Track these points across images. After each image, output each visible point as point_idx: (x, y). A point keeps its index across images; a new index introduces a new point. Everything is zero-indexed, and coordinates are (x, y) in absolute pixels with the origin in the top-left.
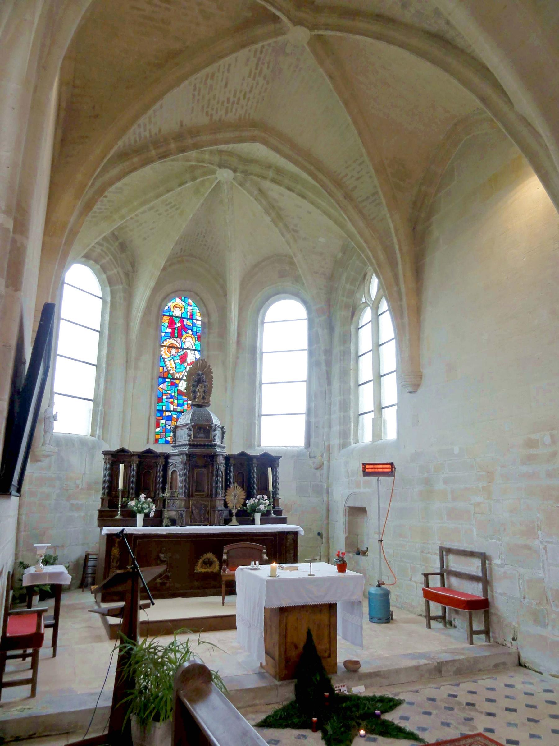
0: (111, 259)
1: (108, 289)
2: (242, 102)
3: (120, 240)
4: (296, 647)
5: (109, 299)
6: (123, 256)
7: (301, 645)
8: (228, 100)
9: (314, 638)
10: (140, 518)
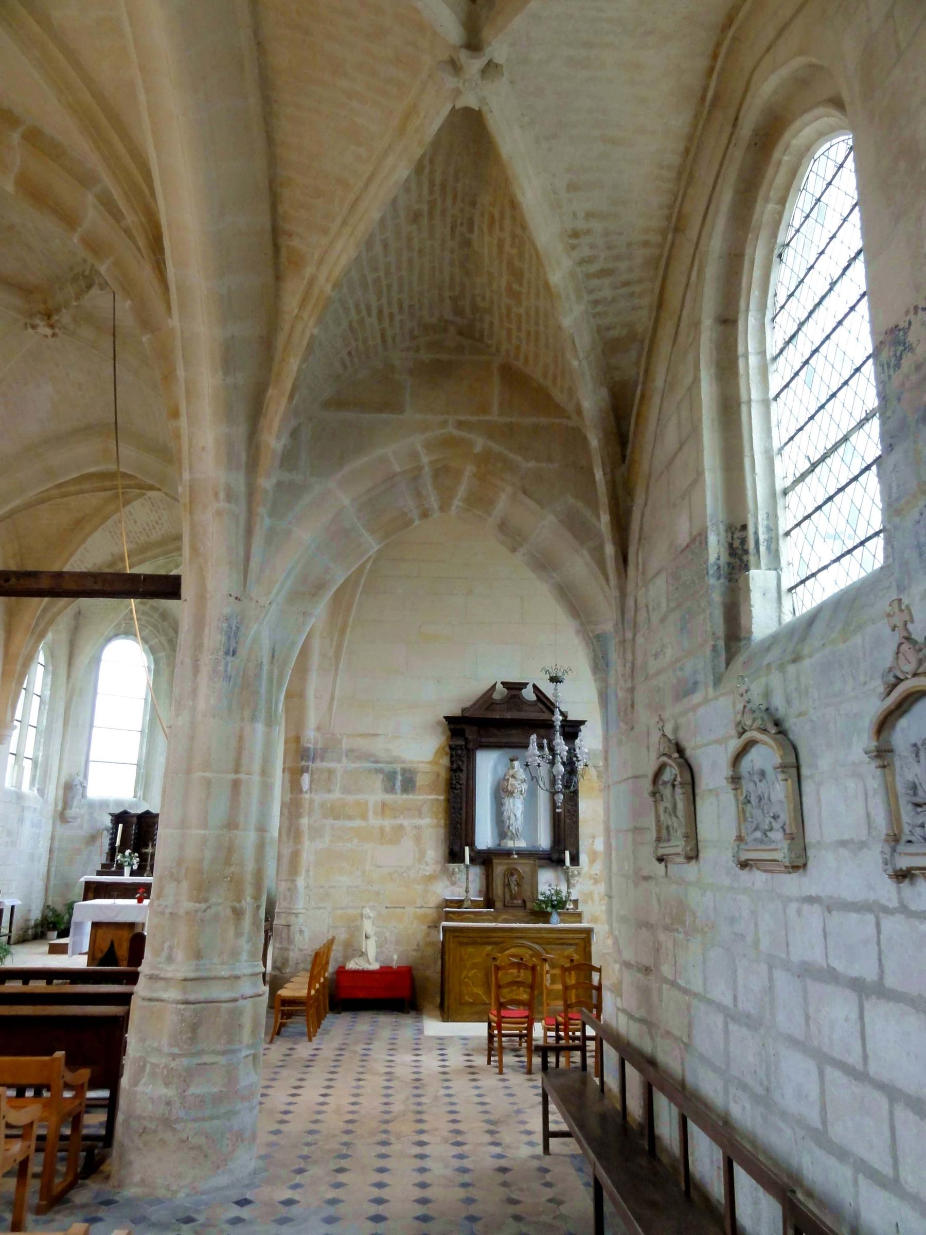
0: (151, 631)
1: (152, 658)
2: (157, 527)
3: (161, 610)
4: (102, 952)
5: (153, 667)
6: (165, 624)
7: (105, 950)
8: (144, 529)
9: (116, 945)
10: (127, 870)
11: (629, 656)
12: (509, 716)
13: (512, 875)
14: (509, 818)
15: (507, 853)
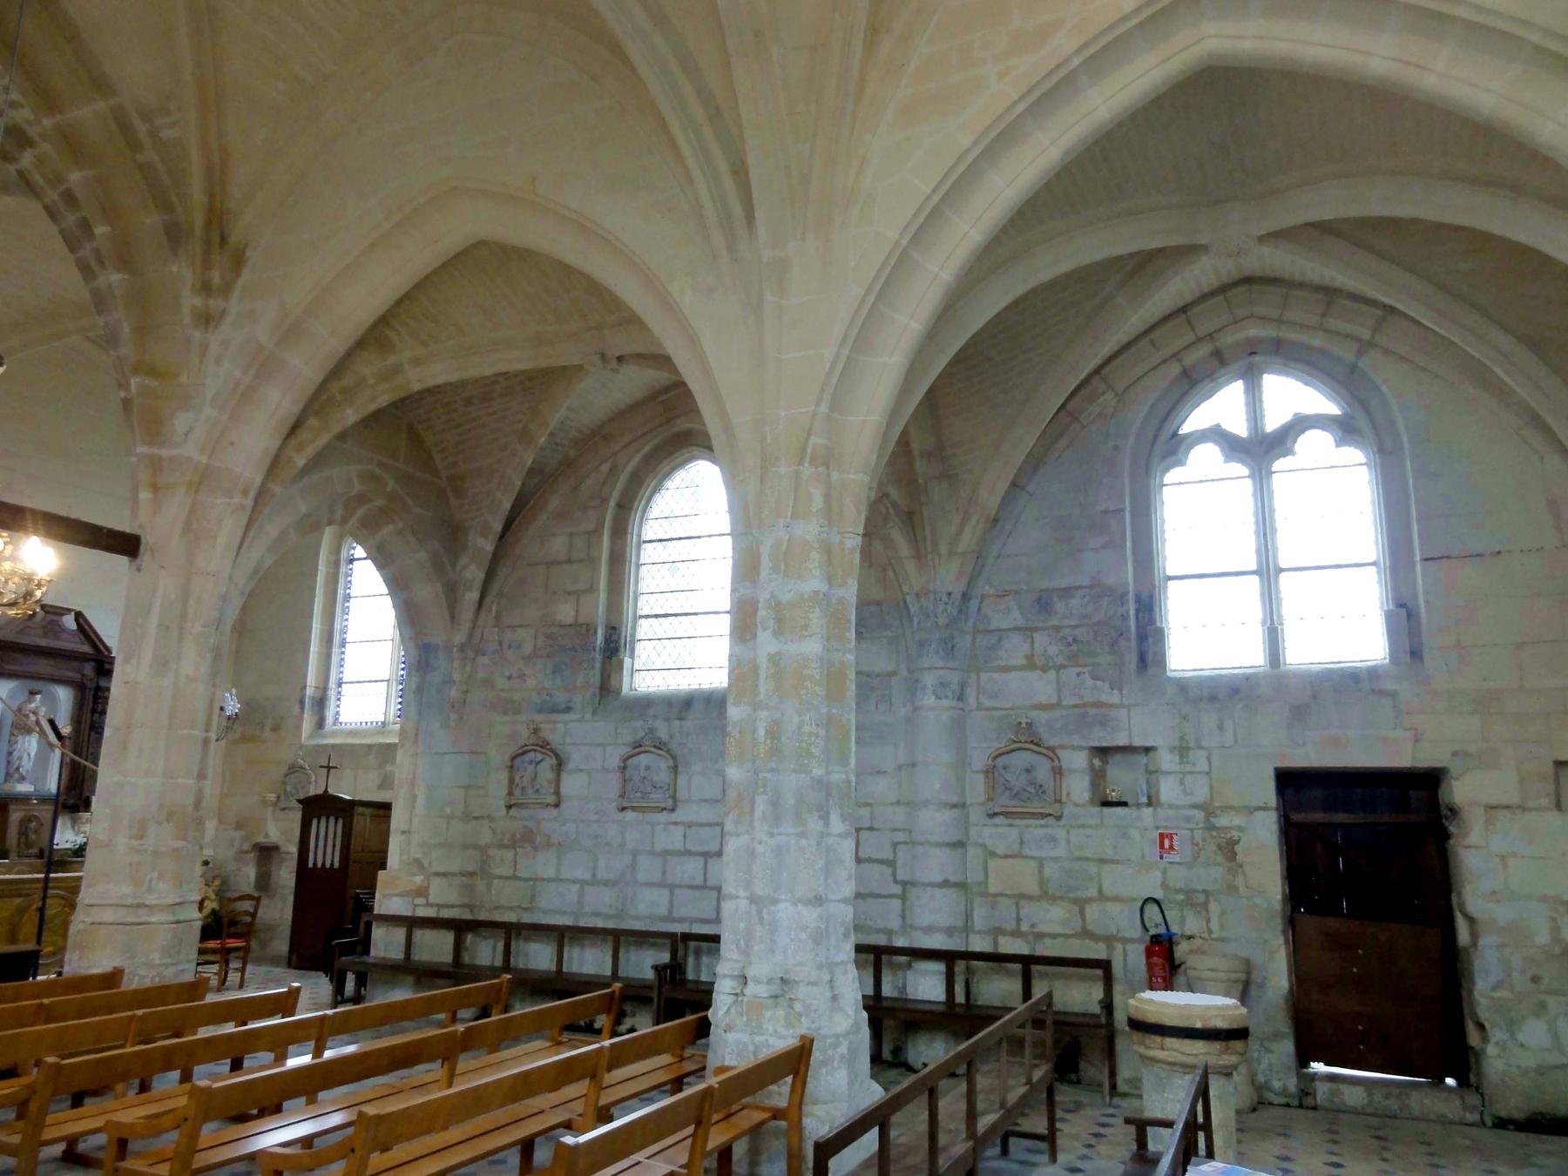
11: (468, 669)
12: (44, 642)
13: (30, 821)
14: (20, 758)
15: (24, 799)
